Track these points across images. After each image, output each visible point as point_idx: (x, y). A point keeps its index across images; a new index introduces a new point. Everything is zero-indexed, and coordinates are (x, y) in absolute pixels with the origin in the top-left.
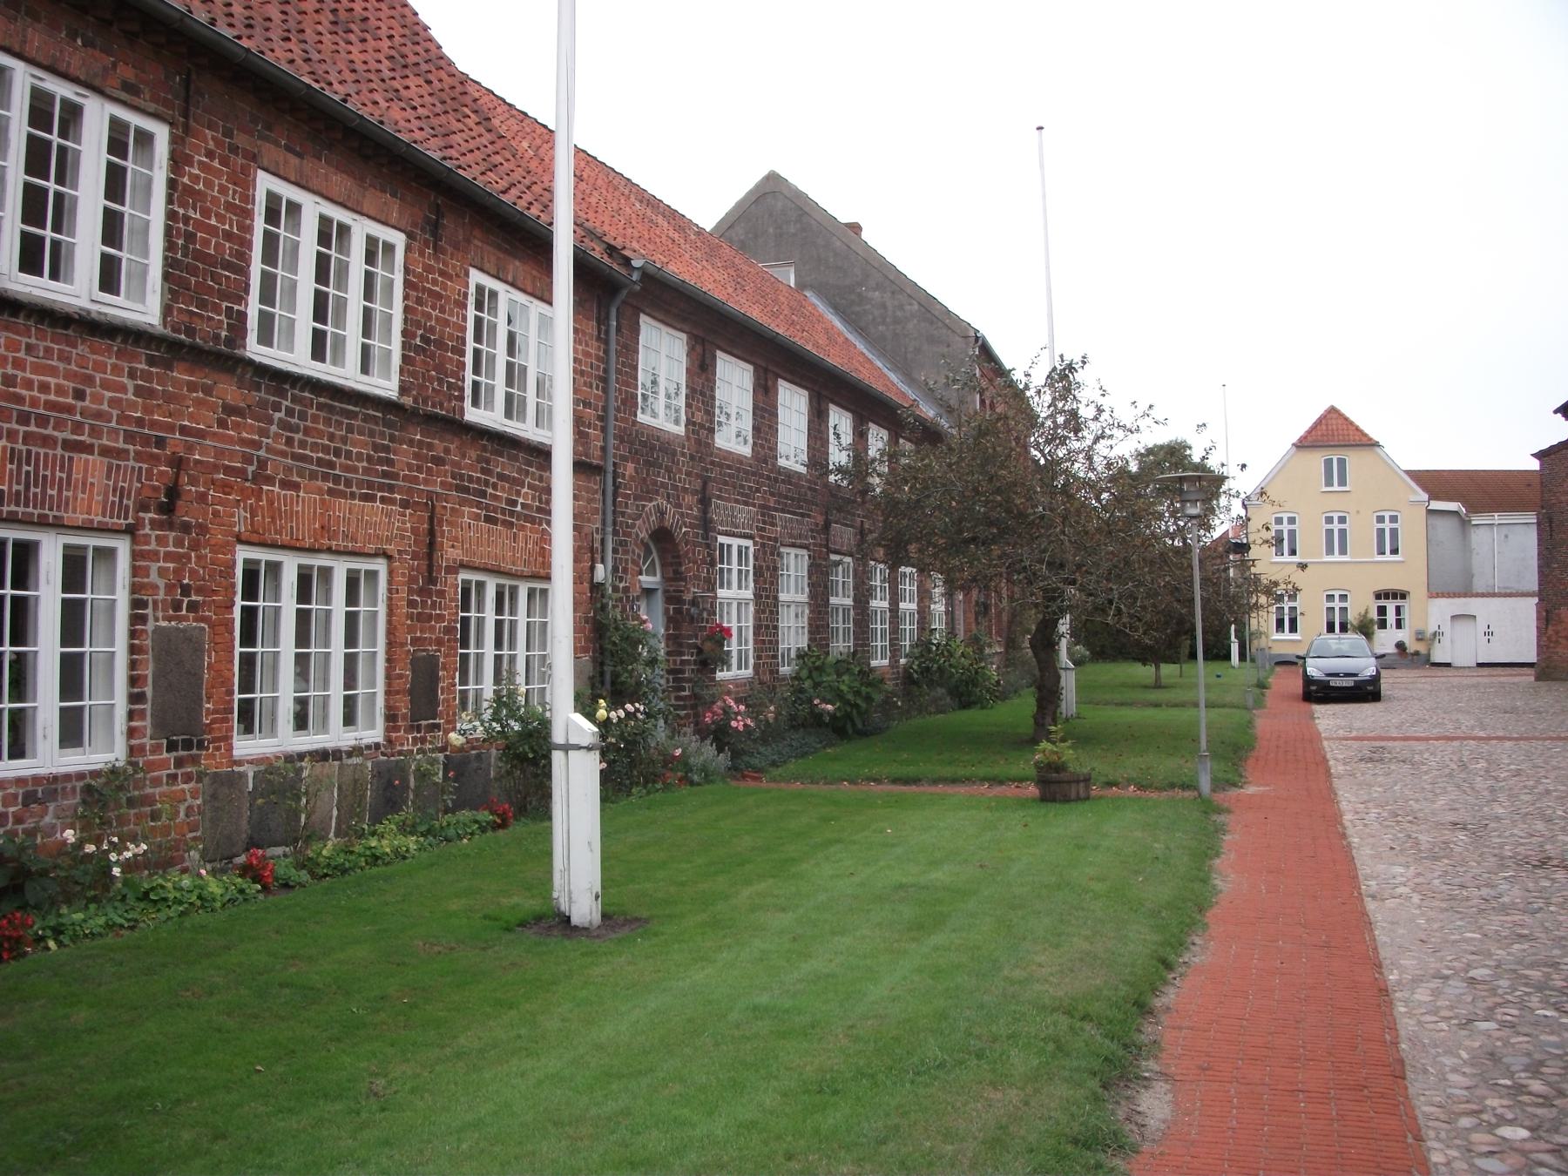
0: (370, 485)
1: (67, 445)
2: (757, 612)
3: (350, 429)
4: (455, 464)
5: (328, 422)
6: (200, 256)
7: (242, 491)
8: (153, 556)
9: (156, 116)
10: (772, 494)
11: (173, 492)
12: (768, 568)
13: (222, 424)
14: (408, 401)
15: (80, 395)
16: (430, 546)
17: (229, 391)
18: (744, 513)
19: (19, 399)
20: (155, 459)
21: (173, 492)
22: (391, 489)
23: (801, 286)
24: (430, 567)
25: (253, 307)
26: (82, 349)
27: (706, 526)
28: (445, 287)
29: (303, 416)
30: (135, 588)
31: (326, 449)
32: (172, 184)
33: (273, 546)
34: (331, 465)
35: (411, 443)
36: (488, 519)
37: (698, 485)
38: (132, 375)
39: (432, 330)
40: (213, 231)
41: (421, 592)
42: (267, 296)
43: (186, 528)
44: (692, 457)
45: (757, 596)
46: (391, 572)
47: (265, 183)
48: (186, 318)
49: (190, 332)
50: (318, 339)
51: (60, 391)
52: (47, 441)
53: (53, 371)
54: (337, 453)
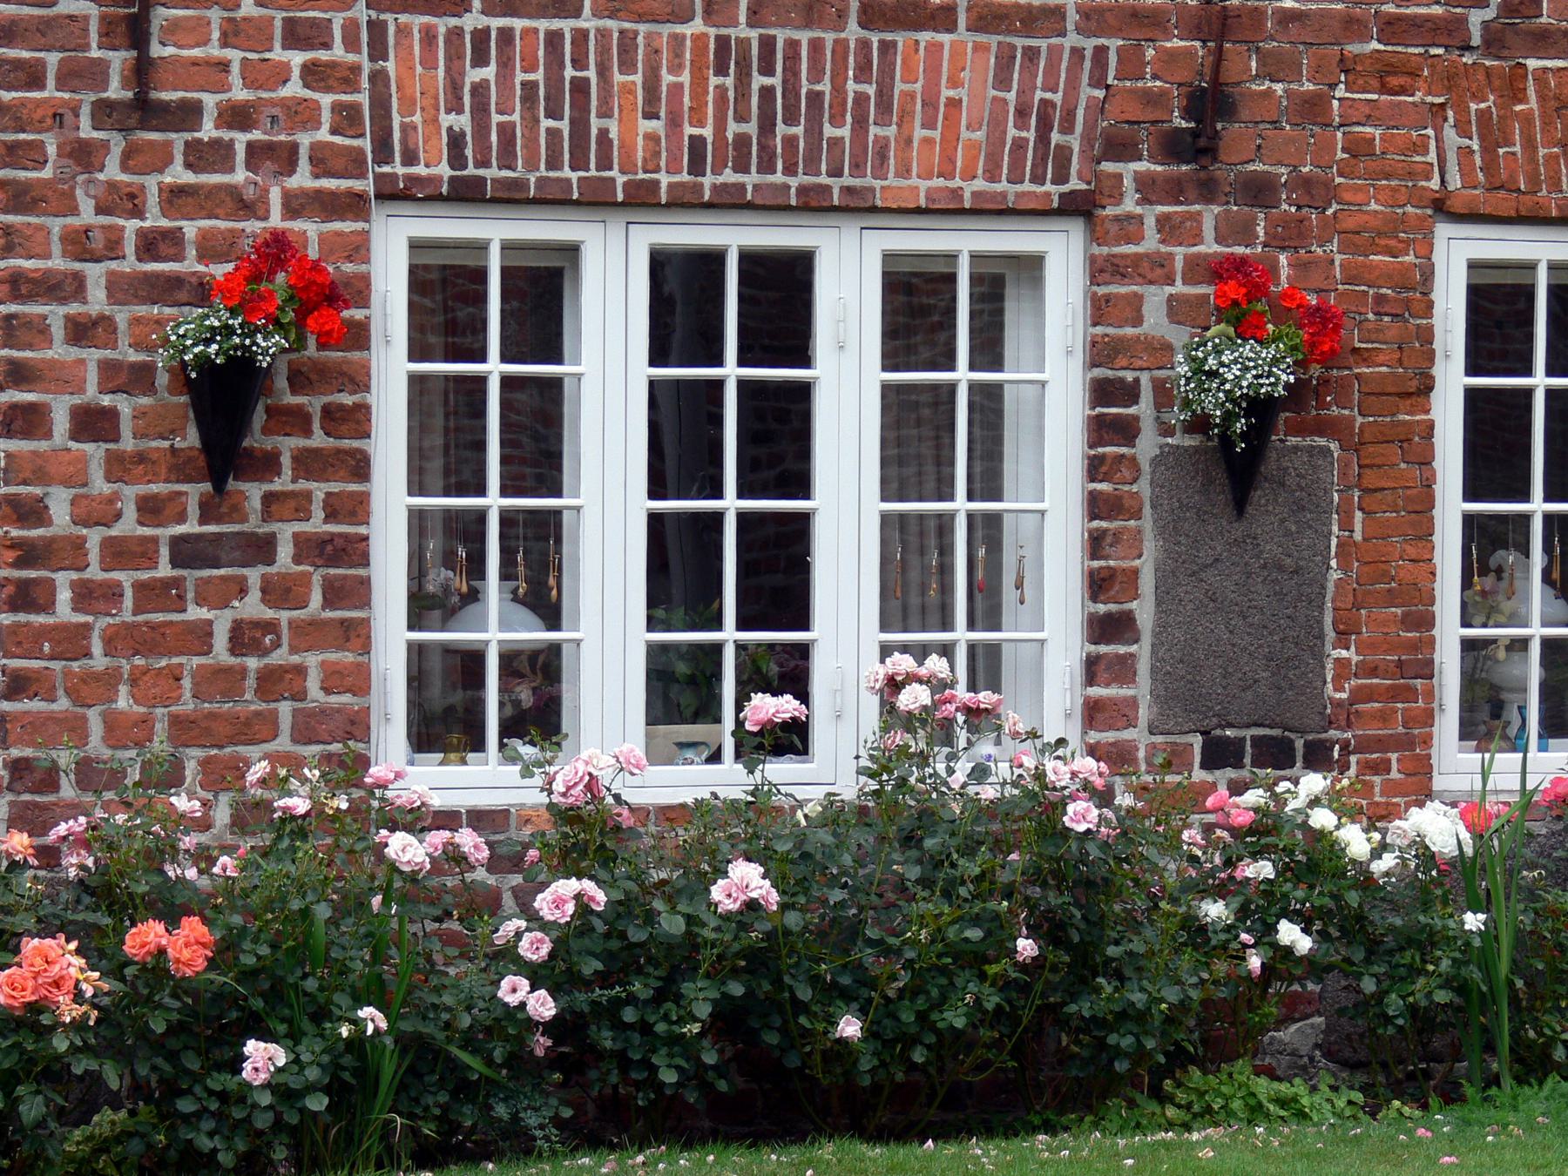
7: (1450, 80)
30: (1099, 353)
43: (1259, 192)
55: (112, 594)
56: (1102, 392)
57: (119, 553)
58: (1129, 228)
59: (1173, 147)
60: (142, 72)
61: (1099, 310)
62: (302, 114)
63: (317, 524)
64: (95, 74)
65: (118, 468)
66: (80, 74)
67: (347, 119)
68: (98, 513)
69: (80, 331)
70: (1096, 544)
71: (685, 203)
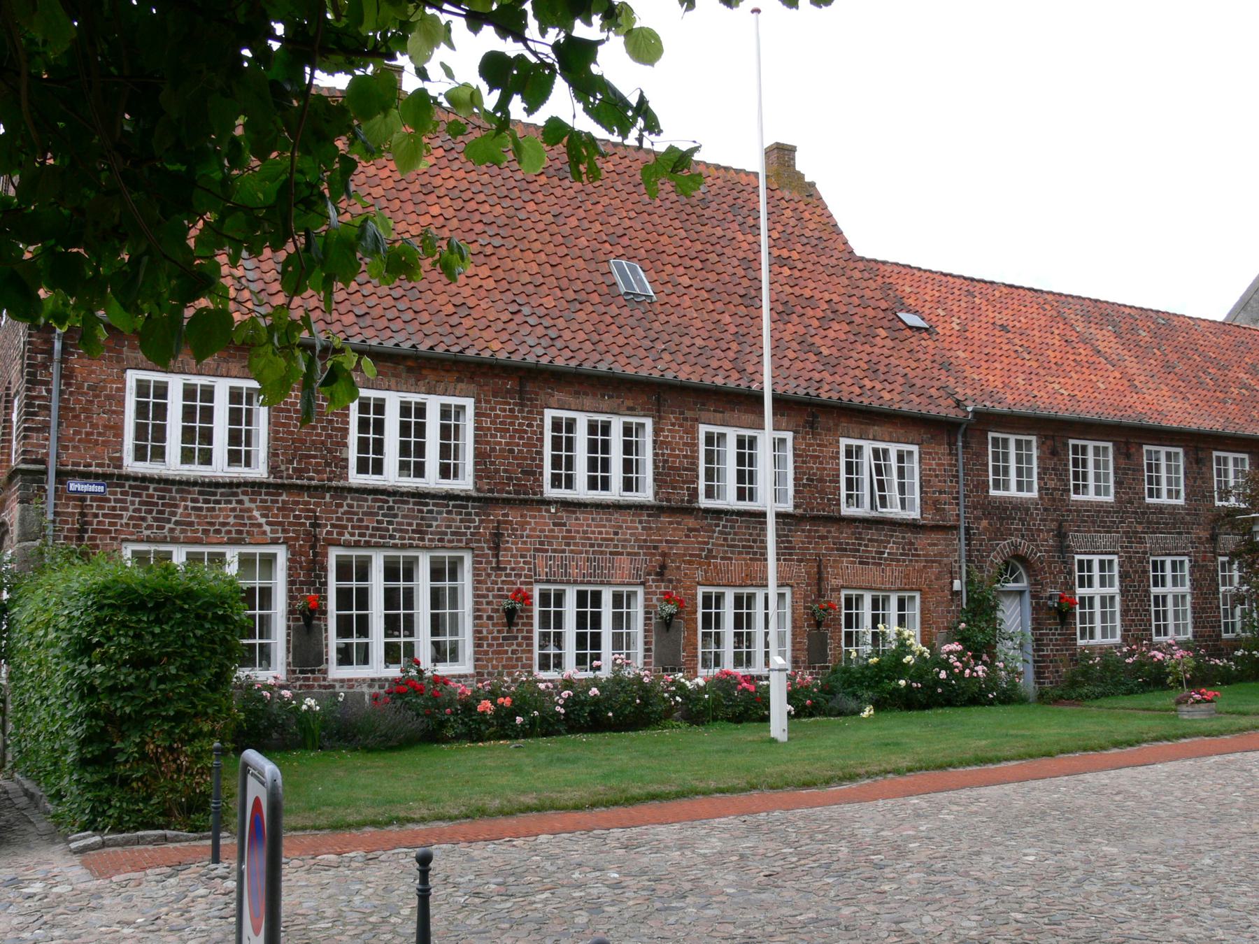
1: (611, 553)
2: (1122, 601)
4: (833, 537)
5: (748, 528)
7: (699, 563)
9: (645, 416)
10: (1140, 523)
11: (663, 567)
14: (800, 511)
15: (616, 533)
16: (820, 579)
17: (691, 522)
18: (1103, 539)
19: (590, 539)
21: (663, 567)
22: (790, 554)
24: (819, 590)
25: (702, 484)
26: (616, 516)
27: (1063, 549)
28: (822, 451)
29: (732, 527)
30: (646, 606)
31: (748, 541)
32: (655, 442)
33: (718, 585)
34: (751, 547)
35: (803, 531)
36: (861, 563)
37: (1054, 525)
38: (640, 522)
39: (815, 474)
40: (678, 456)
43: (670, 581)
44: (1045, 510)
45: (1124, 592)
46: (793, 593)
48: (666, 495)
49: (668, 500)
51: (607, 533)
52: (602, 553)
53: (604, 526)
54: (755, 541)
55: (493, 645)
56: (646, 613)
57: (494, 639)
58: (651, 587)
59: (657, 574)
60: (498, 562)
61: (646, 600)
62: (523, 569)
63: (525, 634)
64: (491, 562)
65: (494, 625)
66: (489, 562)
67: (530, 570)
68: (490, 632)
69: (488, 603)
70: (646, 637)
71: (582, 583)
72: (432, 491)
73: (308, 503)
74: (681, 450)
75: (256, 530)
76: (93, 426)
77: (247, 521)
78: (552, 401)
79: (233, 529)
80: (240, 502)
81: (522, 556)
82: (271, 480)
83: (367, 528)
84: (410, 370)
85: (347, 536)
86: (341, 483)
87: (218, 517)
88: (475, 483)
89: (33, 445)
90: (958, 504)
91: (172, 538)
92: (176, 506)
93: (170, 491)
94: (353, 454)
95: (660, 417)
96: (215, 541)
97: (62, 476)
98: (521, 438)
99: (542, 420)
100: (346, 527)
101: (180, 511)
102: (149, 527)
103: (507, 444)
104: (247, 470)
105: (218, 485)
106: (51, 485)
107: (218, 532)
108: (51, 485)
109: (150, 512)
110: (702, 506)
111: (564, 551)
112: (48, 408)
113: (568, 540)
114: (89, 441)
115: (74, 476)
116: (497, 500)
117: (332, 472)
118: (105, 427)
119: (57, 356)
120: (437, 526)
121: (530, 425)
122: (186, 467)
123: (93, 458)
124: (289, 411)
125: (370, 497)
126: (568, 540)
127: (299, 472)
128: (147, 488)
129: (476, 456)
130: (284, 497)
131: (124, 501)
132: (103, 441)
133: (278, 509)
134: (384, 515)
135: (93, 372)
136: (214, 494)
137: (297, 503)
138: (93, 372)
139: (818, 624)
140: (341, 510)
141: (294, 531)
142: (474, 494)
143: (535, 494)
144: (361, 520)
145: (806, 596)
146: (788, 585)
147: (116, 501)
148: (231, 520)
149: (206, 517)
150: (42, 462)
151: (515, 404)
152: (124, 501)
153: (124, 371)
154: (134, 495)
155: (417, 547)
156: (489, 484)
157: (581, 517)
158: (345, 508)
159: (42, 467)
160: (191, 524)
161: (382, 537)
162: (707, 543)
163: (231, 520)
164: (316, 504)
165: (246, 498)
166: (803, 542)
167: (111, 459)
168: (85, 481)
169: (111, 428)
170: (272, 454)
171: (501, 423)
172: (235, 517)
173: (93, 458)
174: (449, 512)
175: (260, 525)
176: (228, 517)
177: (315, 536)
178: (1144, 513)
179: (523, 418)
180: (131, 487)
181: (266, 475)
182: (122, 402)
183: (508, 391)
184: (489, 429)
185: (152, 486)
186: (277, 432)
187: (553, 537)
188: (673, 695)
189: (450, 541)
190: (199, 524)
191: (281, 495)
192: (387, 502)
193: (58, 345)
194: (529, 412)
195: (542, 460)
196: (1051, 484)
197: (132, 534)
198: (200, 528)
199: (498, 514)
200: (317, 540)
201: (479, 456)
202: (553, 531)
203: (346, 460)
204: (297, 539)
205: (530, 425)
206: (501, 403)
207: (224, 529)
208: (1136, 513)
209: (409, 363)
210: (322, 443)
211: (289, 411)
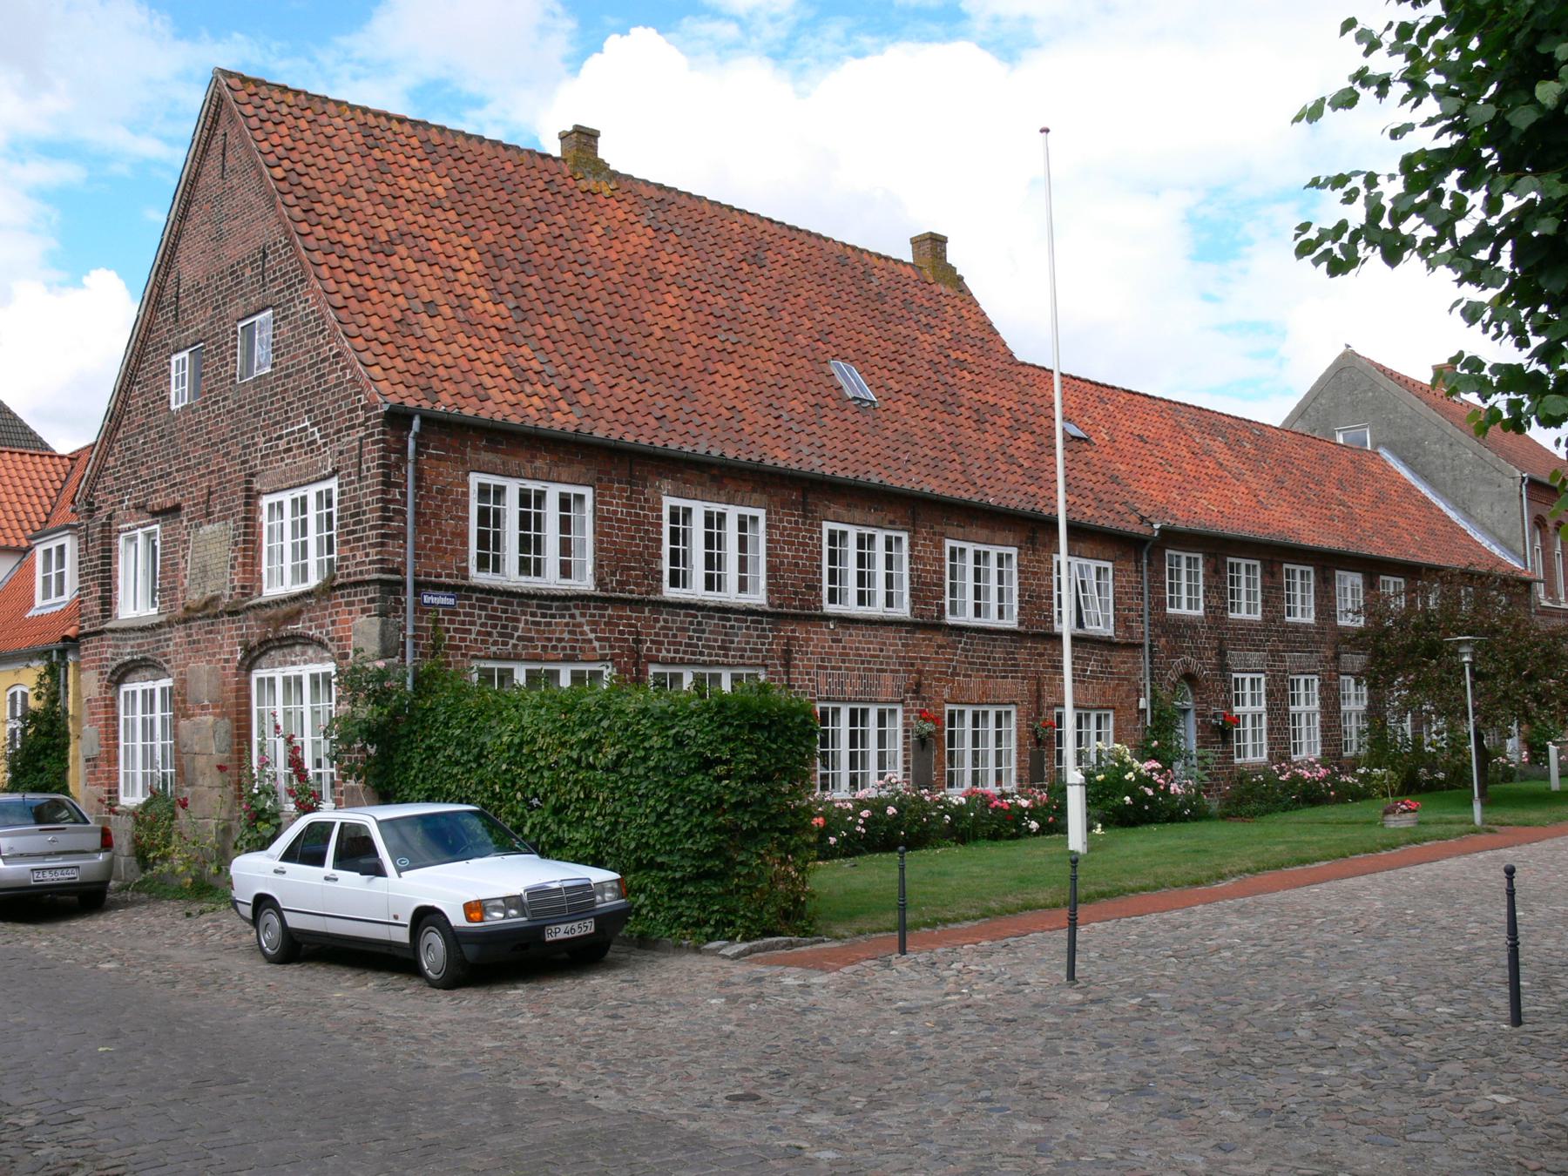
0: (1005, 671)
1: (879, 671)
2: (1269, 719)
3: (994, 647)
4: (1049, 655)
5: (983, 645)
6: (924, 584)
7: (947, 681)
8: (911, 711)
9: (903, 530)
10: (1281, 642)
11: (919, 684)
12: (1278, 691)
13: (937, 653)
14: (1023, 628)
15: (881, 650)
16: (1039, 697)
17: (939, 639)
18: (1254, 658)
19: (860, 655)
20: (910, 672)
21: (919, 684)
22: (1016, 672)
23: (1376, 445)
24: (1038, 708)
25: (947, 600)
26: (881, 632)
27: (1223, 668)
28: (1039, 568)
29: (972, 644)
30: (905, 725)
31: (984, 658)
32: (911, 556)
33: (961, 703)
34: (986, 664)
35: (1026, 648)
37: (1215, 643)
38: (900, 639)
40: (928, 571)
41: (1034, 719)
42: (953, 593)
43: (924, 699)
44: (1210, 628)
45: (1270, 710)
46: (1018, 711)
47: (949, 543)
49: (922, 617)
50: (977, 608)
51: (874, 650)
52: (871, 670)
53: (871, 643)
54: (989, 658)
62: (808, 686)
66: (781, 680)
70: (905, 756)
71: (855, 701)
72: (735, 606)
73: (630, 618)
74: (931, 565)
75: (587, 646)
76: (443, 533)
77: (579, 637)
78: (830, 513)
79: (568, 645)
80: (572, 616)
81: (808, 673)
82: (598, 593)
83: (680, 644)
84: (713, 478)
85: (664, 653)
86: (658, 597)
87: (553, 632)
88: (768, 598)
89: (389, 553)
90: (1142, 622)
91: (515, 654)
92: (518, 620)
93: (511, 604)
94: (666, 566)
95: (915, 532)
96: (552, 658)
97: (419, 587)
98: (804, 551)
99: (821, 533)
100: (662, 643)
101: (521, 625)
102: (495, 643)
103: (794, 557)
104: (537, 579)
105: (554, 598)
106: (409, 598)
107: (555, 648)
108: (409, 598)
109: (494, 627)
110: (949, 622)
111: (840, 668)
112: (403, 513)
113: (844, 657)
114: (439, 549)
115: (427, 588)
116: (786, 615)
117: (649, 585)
118: (453, 534)
119: (411, 455)
120: (739, 642)
121: (811, 538)
122: (524, 578)
123: (444, 567)
124: (611, 520)
125: (682, 612)
126: (844, 657)
127: (622, 584)
128: (491, 601)
129: (768, 570)
130: (610, 612)
131: (471, 615)
132: (452, 550)
133: (605, 623)
134: (694, 631)
135: (440, 474)
136: (550, 608)
137: (620, 618)
138: (440, 474)
139: (1039, 742)
140: (658, 625)
141: (620, 647)
142: (767, 608)
143: (816, 609)
144: (675, 636)
145: (1029, 714)
146: (1014, 703)
147: (466, 614)
148: (566, 636)
149: (544, 632)
150: (396, 571)
151: (799, 516)
152: (471, 615)
153: (467, 475)
154: (481, 608)
155: (723, 664)
156: (779, 598)
157: (854, 632)
158: (662, 623)
159: (398, 577)
160: (531, 639)
161: (693, 653)
162: (952, 660)
163: (566, 636)
164: (638, 619)
165: (577, 612)
166: (1026, 660)
167: (459, 569)
168: (437, 593)
169: (459, 535)
170: (598, 566)
171: (788, 535)
172: (569, 632)
173: (444, 567)
174: (748, 628)
175: (590, 641)
176: (562, 632)
177: (638, 653)
178: (1284, 632)
179: (806, 530)
180: (477, 600)
181: (592, 588)
182: (466, 508)
183: (793, 503)
184: (778, 541)
185: (496, 599)
186: (601, 542)
187: (832, 654)
188: (943, 813)
189: (750, 658)
190: (538, 640)
191: (606, 609)
192: (696, 617)
193: (411, 445)
194: (811, 525)
195: (821, 574)
196: (1214, 602)
197: (480, 650)
198: (540, 644)
199: (787, 629)
200: (639, 656)
201: (772, 570)
202: (830, 647)
203: (661, 572)
204: (621, 656)
205: (811, 538)
206: (787, 515)
207: (560, 645)
208: (1277, 631)
209: (715, 472)
210: (641, 554)
211: (611, 520)
